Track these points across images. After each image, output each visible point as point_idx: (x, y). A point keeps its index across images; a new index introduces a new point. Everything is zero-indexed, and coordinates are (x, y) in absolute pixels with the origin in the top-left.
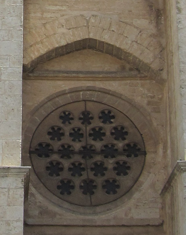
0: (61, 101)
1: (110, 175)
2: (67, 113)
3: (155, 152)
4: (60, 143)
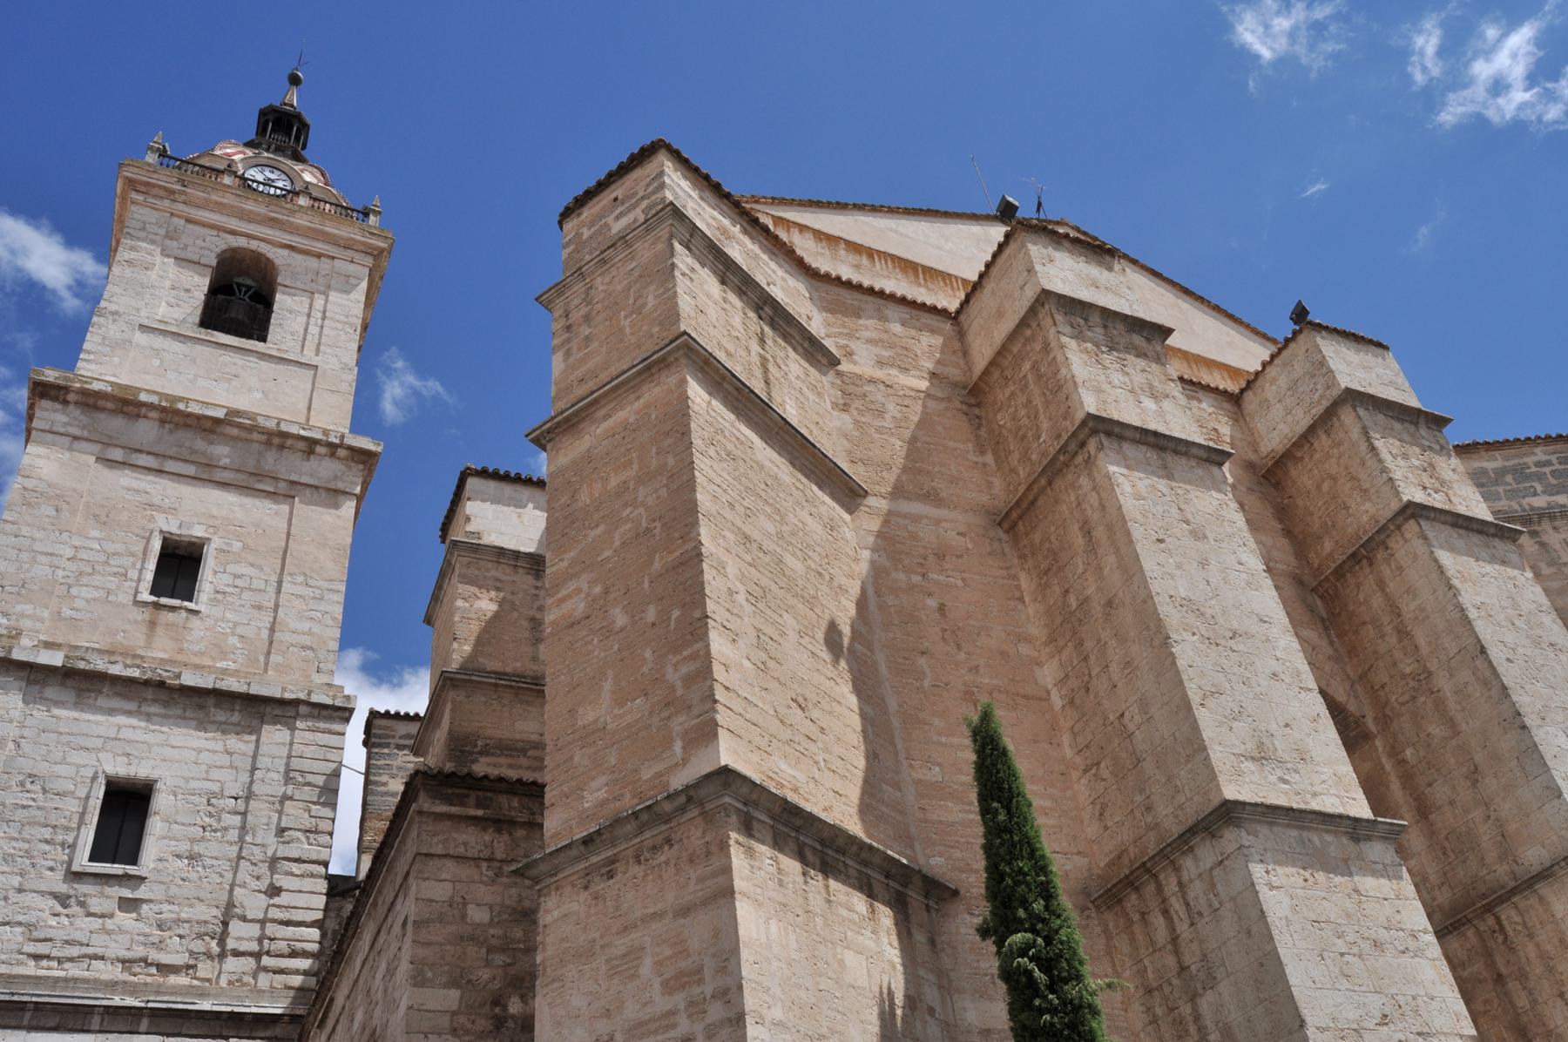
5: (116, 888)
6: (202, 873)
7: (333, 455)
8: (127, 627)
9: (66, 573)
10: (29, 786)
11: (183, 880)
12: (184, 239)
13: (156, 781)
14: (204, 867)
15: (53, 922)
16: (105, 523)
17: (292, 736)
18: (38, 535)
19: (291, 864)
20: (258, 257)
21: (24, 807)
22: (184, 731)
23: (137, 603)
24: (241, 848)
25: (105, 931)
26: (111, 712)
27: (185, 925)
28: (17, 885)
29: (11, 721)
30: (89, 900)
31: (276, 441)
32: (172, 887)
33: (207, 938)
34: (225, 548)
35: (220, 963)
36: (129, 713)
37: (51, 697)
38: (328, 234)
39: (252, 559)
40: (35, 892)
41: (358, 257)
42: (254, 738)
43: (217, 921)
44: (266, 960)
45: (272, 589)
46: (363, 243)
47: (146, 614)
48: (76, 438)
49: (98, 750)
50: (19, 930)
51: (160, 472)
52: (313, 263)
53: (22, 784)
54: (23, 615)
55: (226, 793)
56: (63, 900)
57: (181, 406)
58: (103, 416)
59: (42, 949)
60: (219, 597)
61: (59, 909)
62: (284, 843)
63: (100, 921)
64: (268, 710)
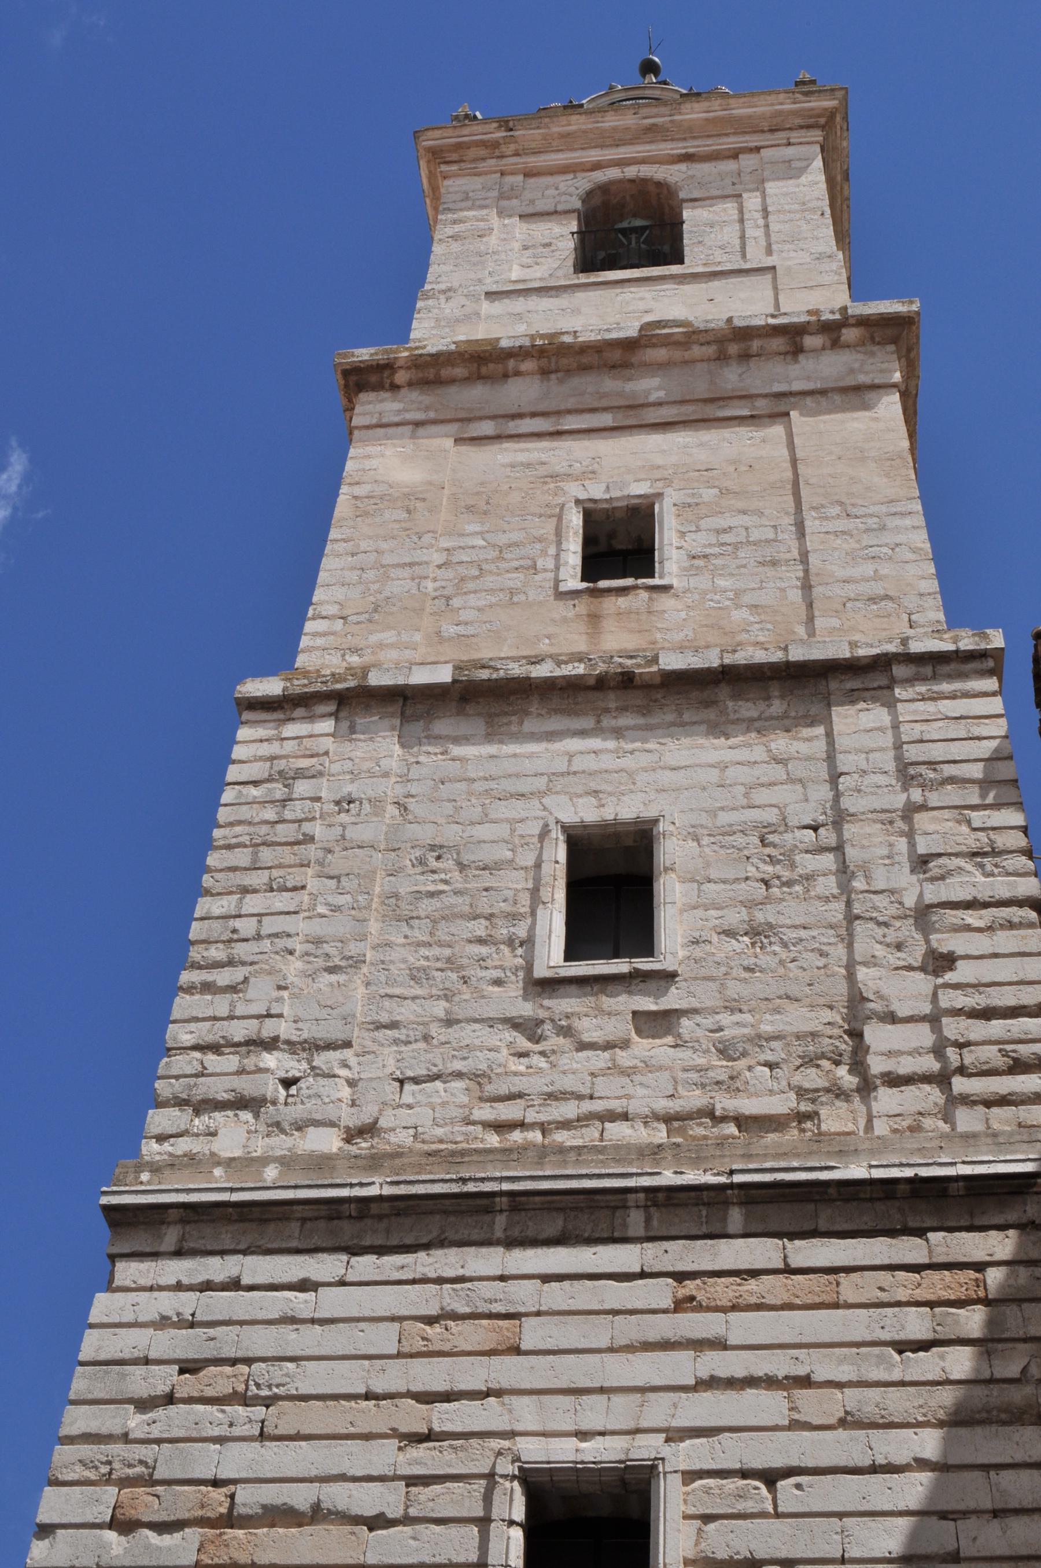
5: (623, 998)
6: (784, 955)
7: (836, 344)
8: (551, 630)
9: (438, 584)
10: (433, 864)
11: (748, 969)
13: (656, 821)
14: (785, 945)
15: (519, 1066)
16: (485, 513)
17: (894, 715)
18: (384, 546)
19: (960, 913)
20: (641, 184)
21: (432, 895)
22: (686, 741)
23: (561, 595)
24: (849, 903)
25: (615, 1069)
26: (551, 736)
27: (774, 1044)
28: (442, 1015)
29: (386, 775)
30: (577, 1024)
31: (733, 349)
32: (730, 984)
33: (825, 1064)
34: (689, 500)
35: (866, 1099)
36: (582, 733)
37: (444, 733)
38: (739, 119)
39: (740, 505)
40: (476, 1021)
41: (795, 136)
42: (820, 730)
43: (837, 1032)
44: (960, 1083)
45: (788, 536)
46: (795, 113)
47: (583, 606)
48: (418, 424)
49: (541, 794)
50: (458, 1085)
51: (558, 434)
52: (731, 166)
53: (421, 862)
54: (381, 646)
55: (793, 821)
56: (530, 1028)
58: (453, 389)
60: (697, 562)
61: (523, 1043)
62: (933, 879)
63: (606, 1055)
64: (833, 685)
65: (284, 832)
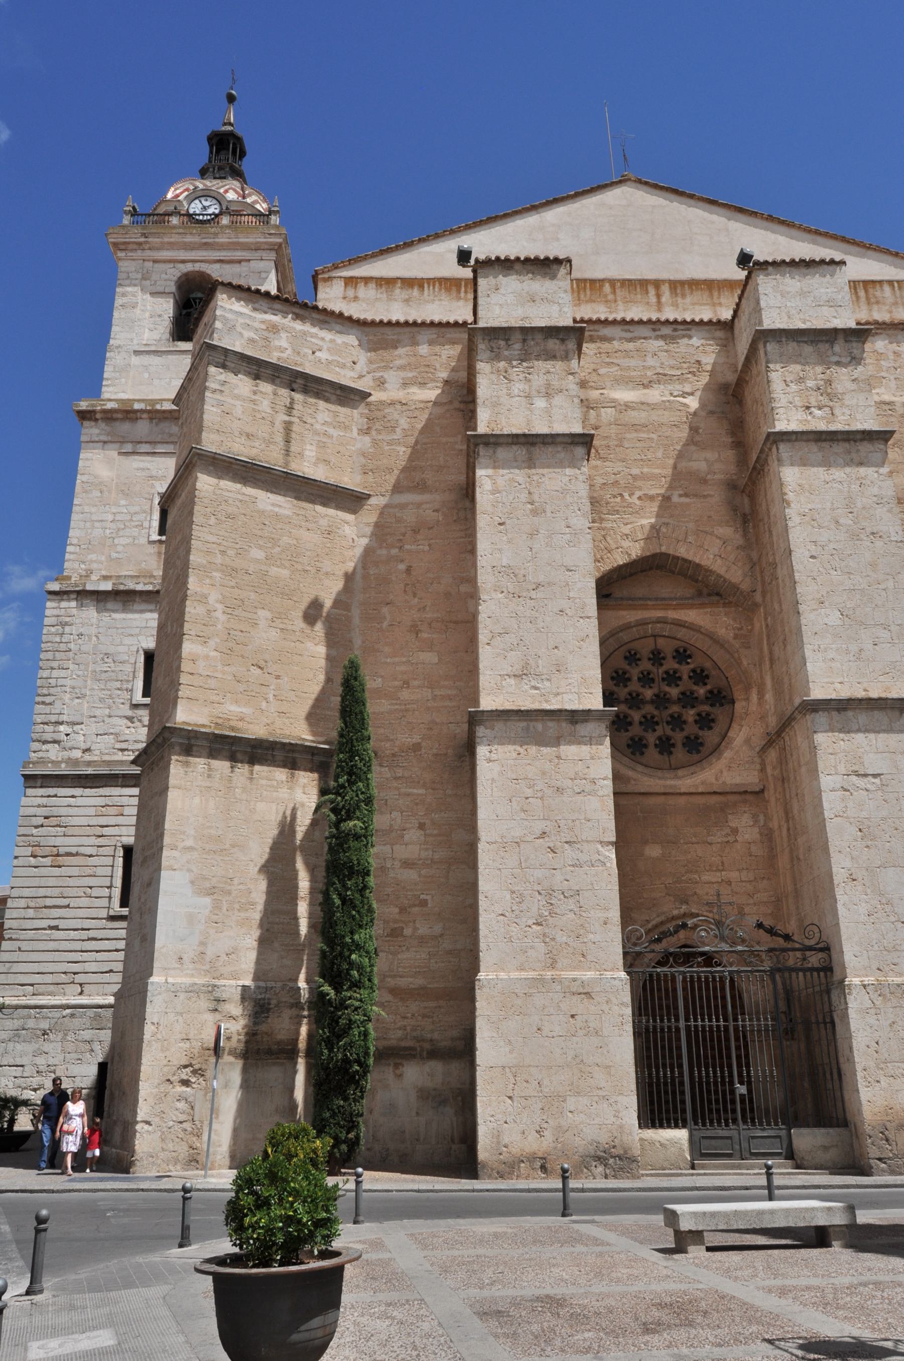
0: (625, 636)
1: (691, 729)
2: (633, 652)
3: (747, 699)
4: (627, 690)
10: (106, 660)
12: (155, 277)
18: (93, 510)
21: (106, 672)
26: (142, 611)
38: (242, 243)
41: (265, 254)
46: (266, 243)
48: (105, 442)
49: (137, 635)
50: (112, 737)
54: (92, 561)
56: (130, 719)
57: (158, 407)
58: (117, 424)
59: (124, 746)
61: (130, 724)
65: (63, 647)
